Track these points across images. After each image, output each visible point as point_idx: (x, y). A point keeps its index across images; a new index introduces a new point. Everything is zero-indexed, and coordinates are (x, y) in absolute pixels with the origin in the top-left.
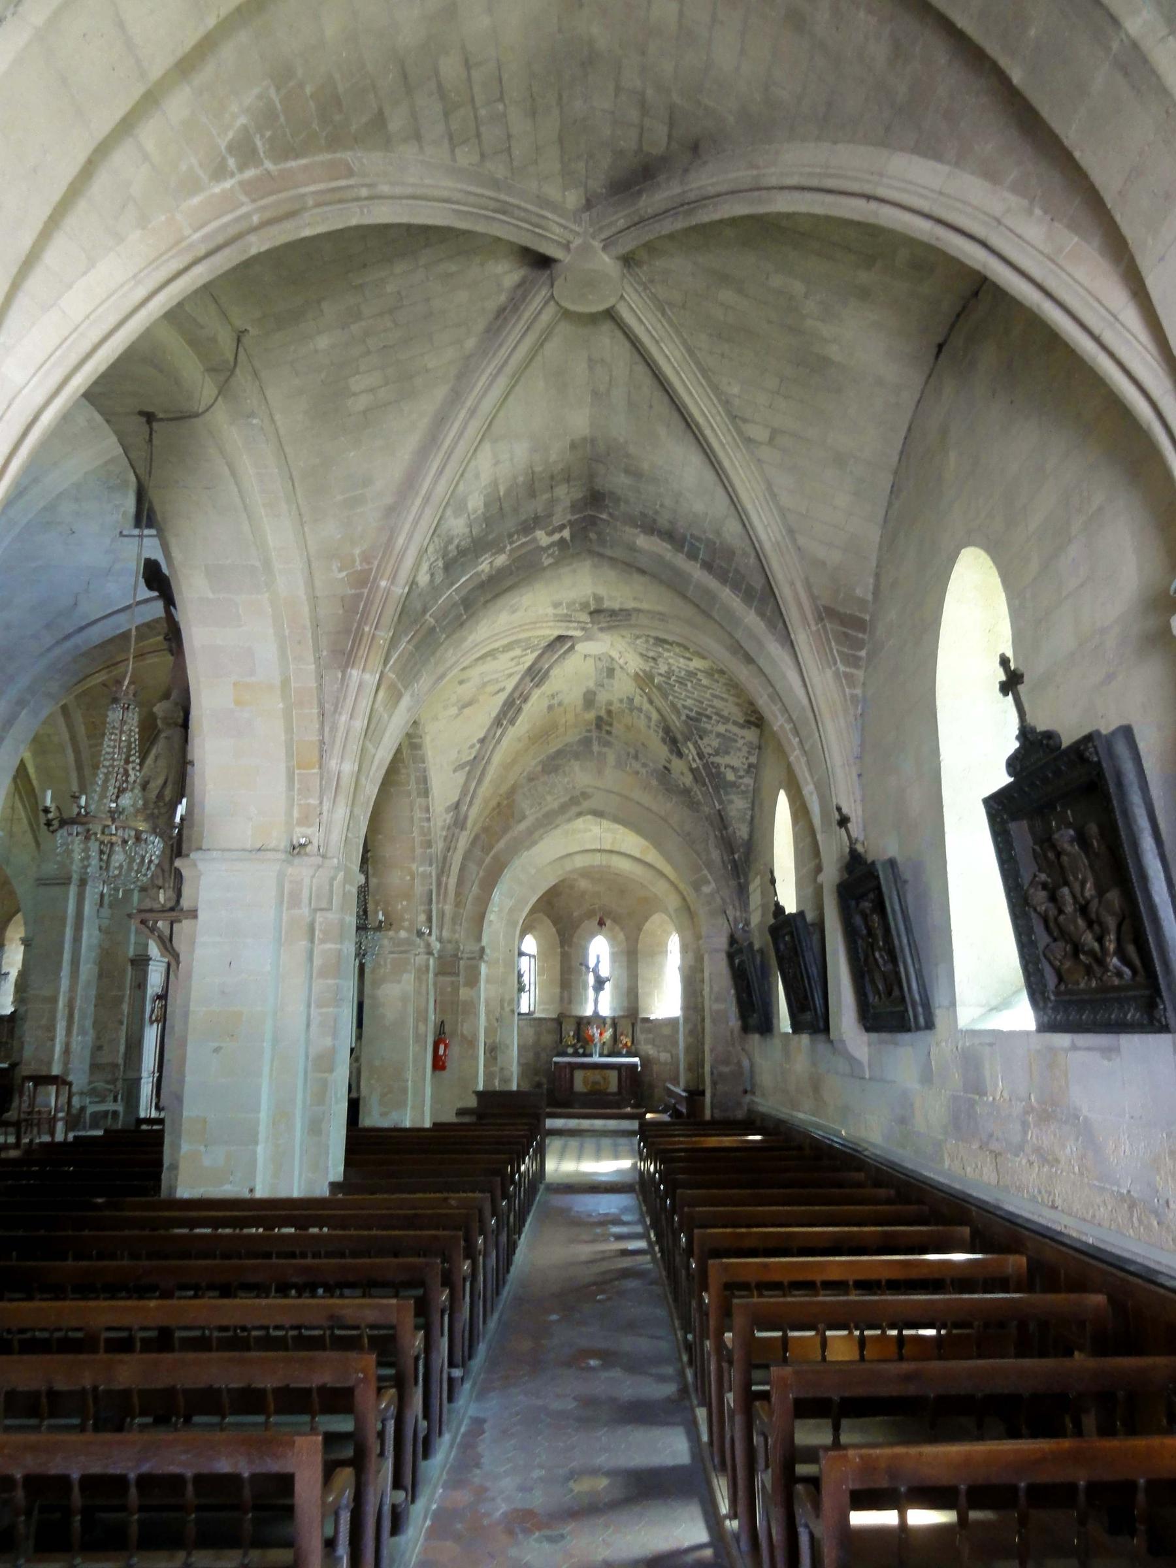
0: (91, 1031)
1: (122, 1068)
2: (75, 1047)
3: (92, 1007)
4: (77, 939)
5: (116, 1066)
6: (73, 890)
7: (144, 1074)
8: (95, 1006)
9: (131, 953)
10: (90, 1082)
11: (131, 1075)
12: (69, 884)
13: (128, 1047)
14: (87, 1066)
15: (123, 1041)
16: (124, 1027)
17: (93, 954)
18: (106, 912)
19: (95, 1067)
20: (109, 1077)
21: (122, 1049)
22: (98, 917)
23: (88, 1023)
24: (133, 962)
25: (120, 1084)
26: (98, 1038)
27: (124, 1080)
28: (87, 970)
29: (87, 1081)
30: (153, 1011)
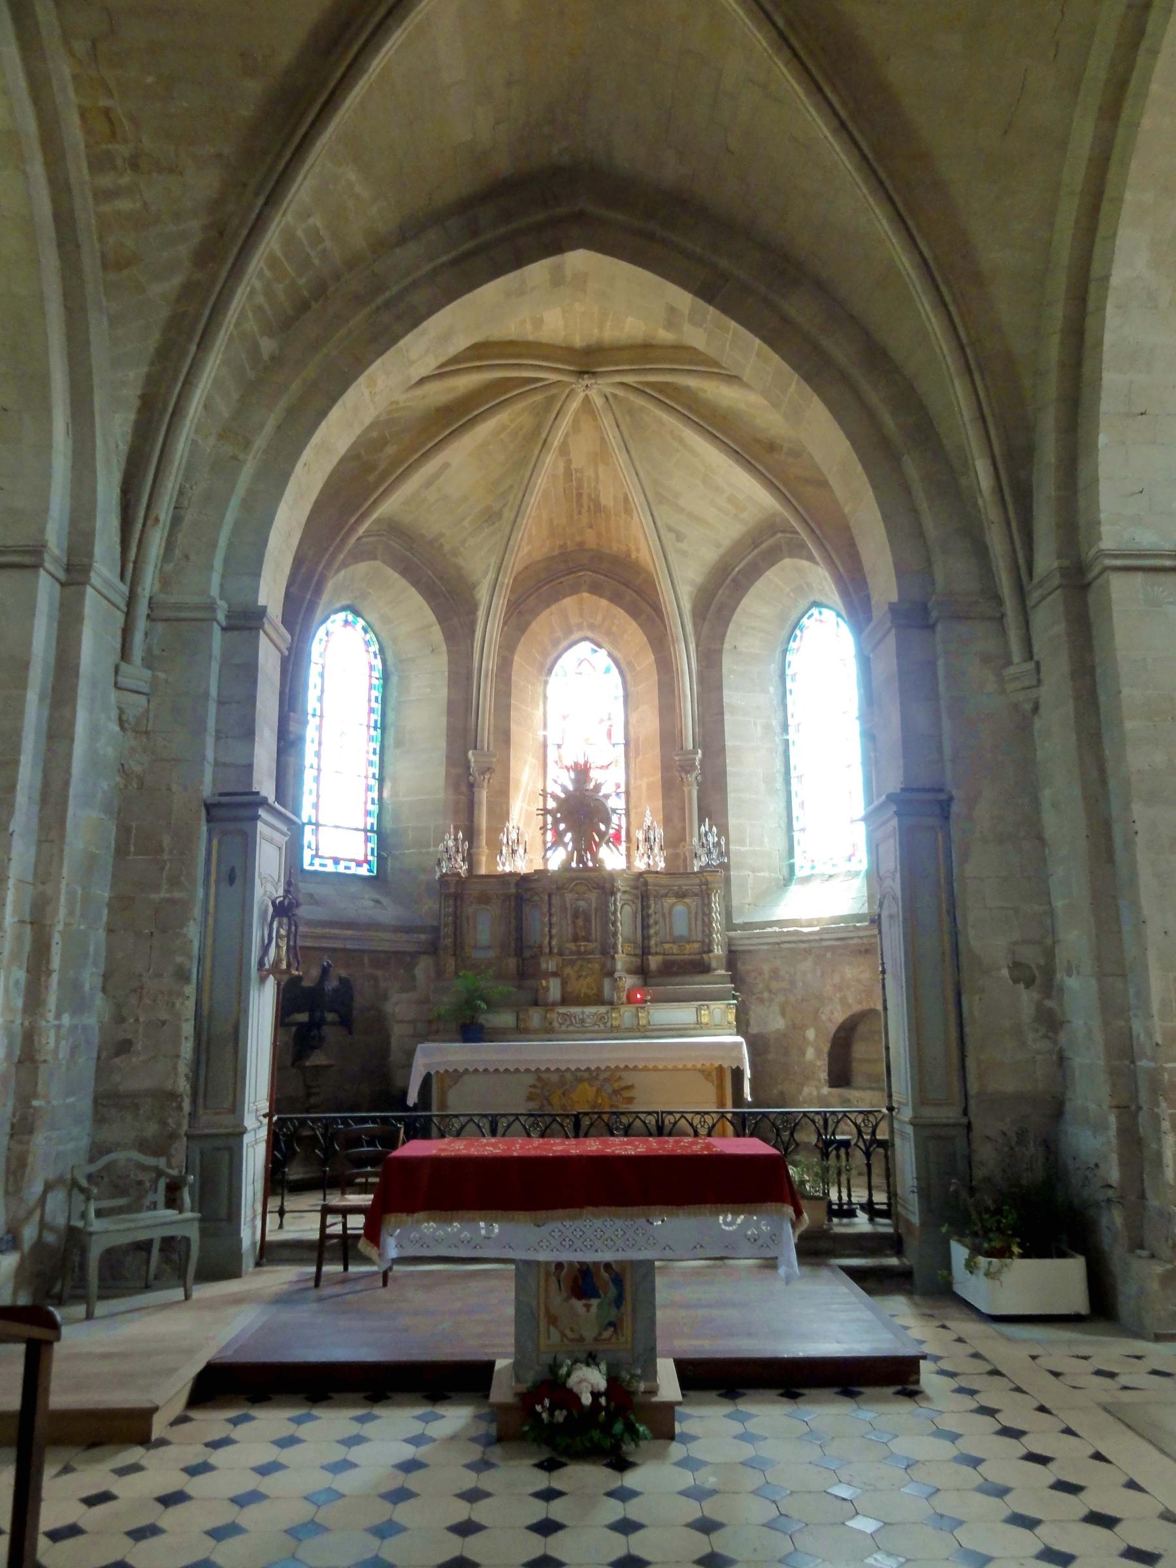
0: (99, 1000)
1: (187, 1105)
2: (51, 1045)
3: (101, 933)
4: (58, 733)
5: (173, 1096)
6: (46, 590)
7: (250, 1122)
8: (110, 931)
9: (207, 790)
10: (97, 1150)
11: (211, 1122)
12: (36, 567)
13: (204, 1043)
14: (84, 1104)
15: (188, 1028)
16: (190, 990)
17: (105, 786)
18: (136, 673)
19: (108, 1102)
20: (151, 1129)
21: (187, 1049)
22: (117, 686)
23: (91, 978)
24: (209, 807)
25: (180, 1149)
26: (119, 1019)
27: (189, 1137)
28: (86, 825)
29: (85, 1142)
30: (265, 949)
